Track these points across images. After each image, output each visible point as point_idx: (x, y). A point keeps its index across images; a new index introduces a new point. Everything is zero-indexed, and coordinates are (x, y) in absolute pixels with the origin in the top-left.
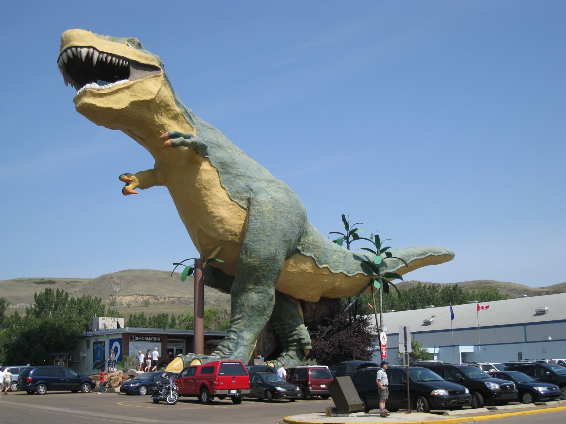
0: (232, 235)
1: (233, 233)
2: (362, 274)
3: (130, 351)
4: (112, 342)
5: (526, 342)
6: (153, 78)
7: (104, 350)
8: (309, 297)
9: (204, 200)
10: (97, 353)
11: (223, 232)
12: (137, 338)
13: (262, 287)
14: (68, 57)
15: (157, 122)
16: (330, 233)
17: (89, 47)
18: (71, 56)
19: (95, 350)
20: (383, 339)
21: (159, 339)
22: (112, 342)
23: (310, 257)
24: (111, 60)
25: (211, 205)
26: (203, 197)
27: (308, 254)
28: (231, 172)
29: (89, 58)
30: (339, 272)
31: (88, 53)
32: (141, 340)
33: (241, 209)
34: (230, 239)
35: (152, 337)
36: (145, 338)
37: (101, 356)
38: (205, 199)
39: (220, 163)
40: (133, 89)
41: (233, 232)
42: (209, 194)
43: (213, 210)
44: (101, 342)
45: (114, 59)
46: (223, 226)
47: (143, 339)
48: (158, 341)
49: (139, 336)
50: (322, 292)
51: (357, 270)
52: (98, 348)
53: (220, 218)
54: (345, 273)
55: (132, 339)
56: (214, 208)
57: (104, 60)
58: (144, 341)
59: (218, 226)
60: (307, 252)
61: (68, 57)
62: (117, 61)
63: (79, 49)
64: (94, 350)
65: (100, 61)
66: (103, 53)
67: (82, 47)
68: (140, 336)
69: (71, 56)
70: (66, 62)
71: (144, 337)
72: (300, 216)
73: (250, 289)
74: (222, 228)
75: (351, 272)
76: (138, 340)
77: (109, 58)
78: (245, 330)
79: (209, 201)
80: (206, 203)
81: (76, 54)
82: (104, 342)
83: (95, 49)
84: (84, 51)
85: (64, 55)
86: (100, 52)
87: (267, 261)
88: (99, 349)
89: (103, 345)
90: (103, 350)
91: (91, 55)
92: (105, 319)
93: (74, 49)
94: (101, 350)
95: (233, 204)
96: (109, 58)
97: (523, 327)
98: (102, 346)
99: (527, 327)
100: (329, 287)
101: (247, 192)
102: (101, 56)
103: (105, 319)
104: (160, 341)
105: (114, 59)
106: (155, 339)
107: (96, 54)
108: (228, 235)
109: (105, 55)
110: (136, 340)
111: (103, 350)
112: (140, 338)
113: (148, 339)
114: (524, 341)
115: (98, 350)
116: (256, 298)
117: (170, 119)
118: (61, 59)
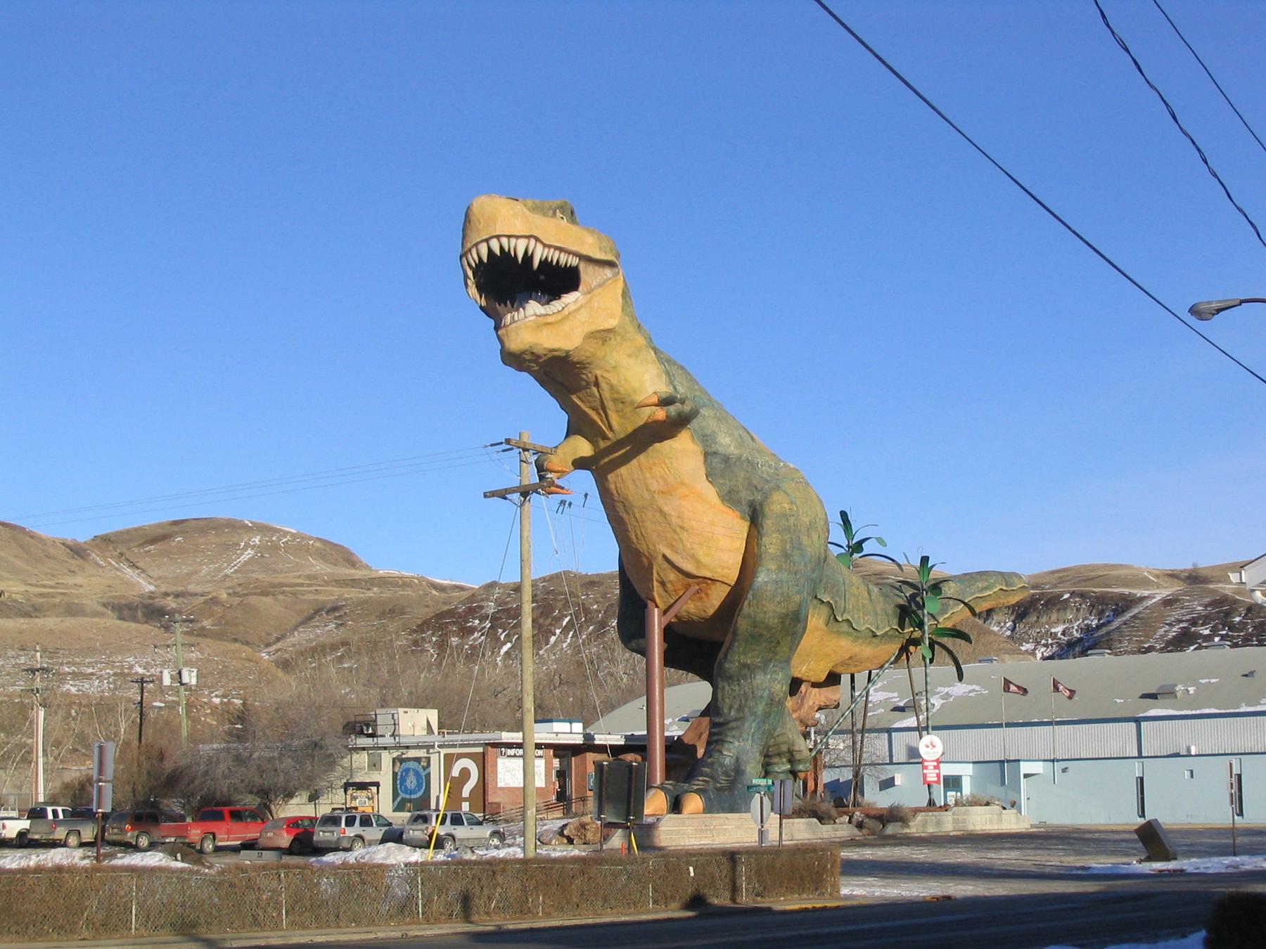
3: (499, 776)
10: (403, 780)
14: (490, 251)
18: (498, 252)
19: (399, 774)
22: (450, 760)
23: (829, 602)
29: (528, 258)
37: (419, 786)
44: (418, 760)
52: (407, 770)
62: (566, 257)
63: (513, 241)
64: (395, 774)
65: (545, 263)
69: (498, 252)
76: (510, 756)
81: (507, 250)
83: (537, 239)
86: (545, 246)
88: (411, 773)
90: (423, 774)
91: (530, 253)
93: (504, 241)
94: (417, 774)
98: (420, 767)
102: (546, 250)
110: (508, 756)
111: (423, 774)
115: (407, 774)
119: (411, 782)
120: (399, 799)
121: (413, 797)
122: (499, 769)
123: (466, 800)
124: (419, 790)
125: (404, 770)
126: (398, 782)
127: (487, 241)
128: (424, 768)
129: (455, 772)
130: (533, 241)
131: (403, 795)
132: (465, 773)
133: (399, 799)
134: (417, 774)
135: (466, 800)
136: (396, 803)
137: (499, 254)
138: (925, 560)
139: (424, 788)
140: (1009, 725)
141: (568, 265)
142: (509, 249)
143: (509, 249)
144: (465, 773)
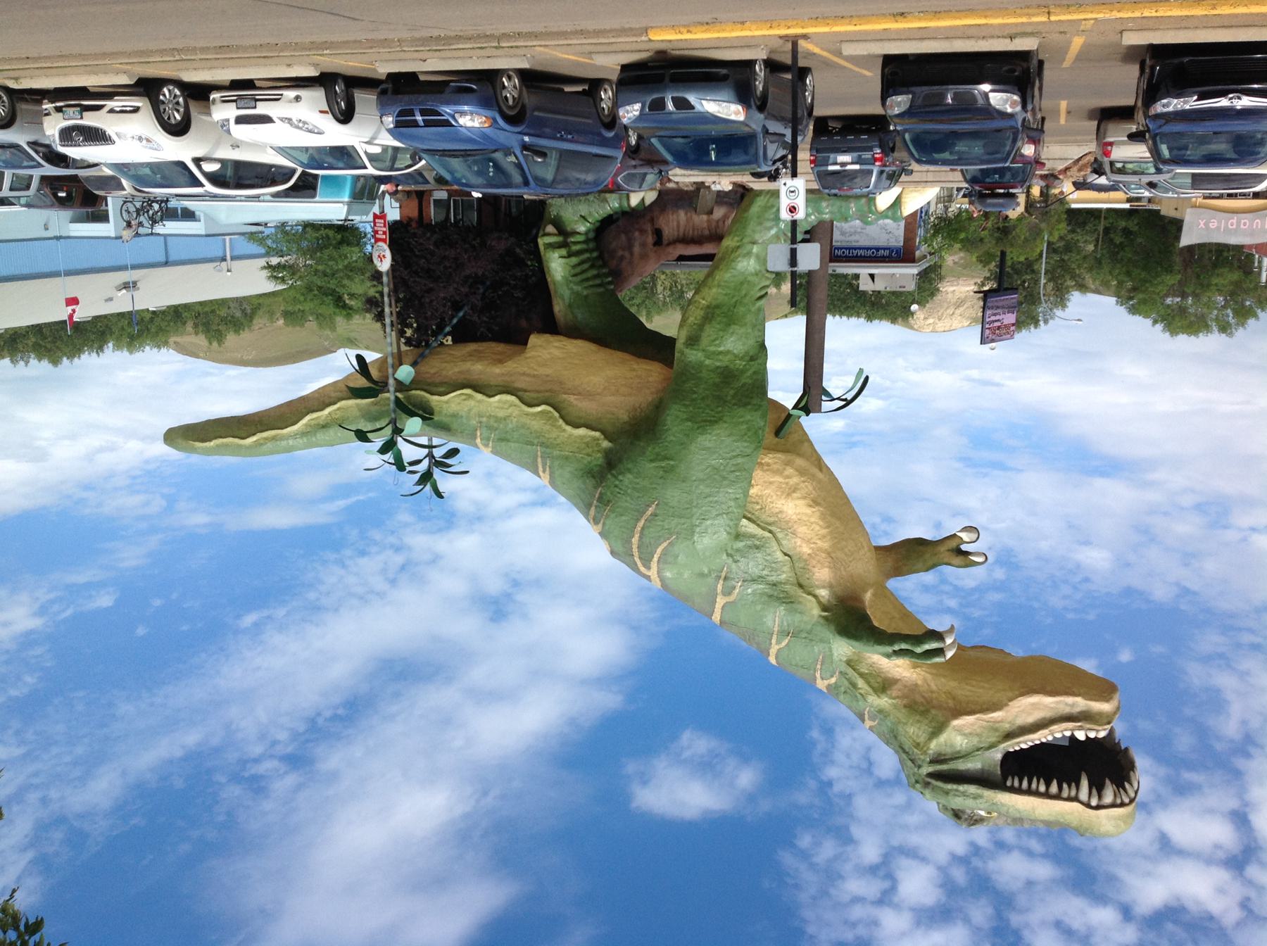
0: (768, 465)
1: (766, 468)
2: (432, 394)
6: (947, 757)
8: (556, 344)
9: (825, 528)
11: (785, 469)
12: (887, 253)
13: (718, 364)
15: (929, 673)
16: (467, 472)
17: (1098, 807)
20: (384, 256)
23: (576, 426)
24: (1048, 785)
25: (813, 520)
26: (831, 533)
27: (582, 431)
28: (767, 587)
30: (497, 398)
31: (1100, 797)
32: (878, 249)
33: (753, 517)
34: (771, 455)
36: (870, 253)
38: (824, 531)
39: (791, 602)
40: (997, 734)
41: (767, 470)
42: (818, 542)
43: (809, 511)
46: (787, 480)
47: (844, 252)
50: (528, 355)
51: (447, 402)
53: (795, 495)
54: (479, 396)
56: (806, 514)
57: (1065, 786)
58: (871, 249)
59: (795, 480)
60: (582, 437)
62: (1034, 786)
66: (1069, 799)
67: (1113, 805)
68: (881, 257)
71: (870, 257)
72: (618, 510)
73: (742, 359)
74: (788, 477)
75: (464, 397)
76: (884, 249)
77: (1025, 784)
78: (752, 275)
79: (818, 528)
80: (821, 523)
81: (1121, 789)
83: (1088, 806)
84: (1108, 797)
86: (1076, 799)
87: (714, 417)
91: (1094, 791)
92: (900, 287)
95: (770, 524)
96: (1054, 788)
100: (515, 365)
101: (738, 550)
102: (1073, 793)
103: (900, 287)
104: (835, 248)
105: (1042, 788)
107: (1084, 795)
108: (775, 463)
109: (1065, 794)
112: (881, 252)
113: (861, 252)
116: (729, 341)
117: (900, 680)
140: (69, 273)
141: (1026, 779)
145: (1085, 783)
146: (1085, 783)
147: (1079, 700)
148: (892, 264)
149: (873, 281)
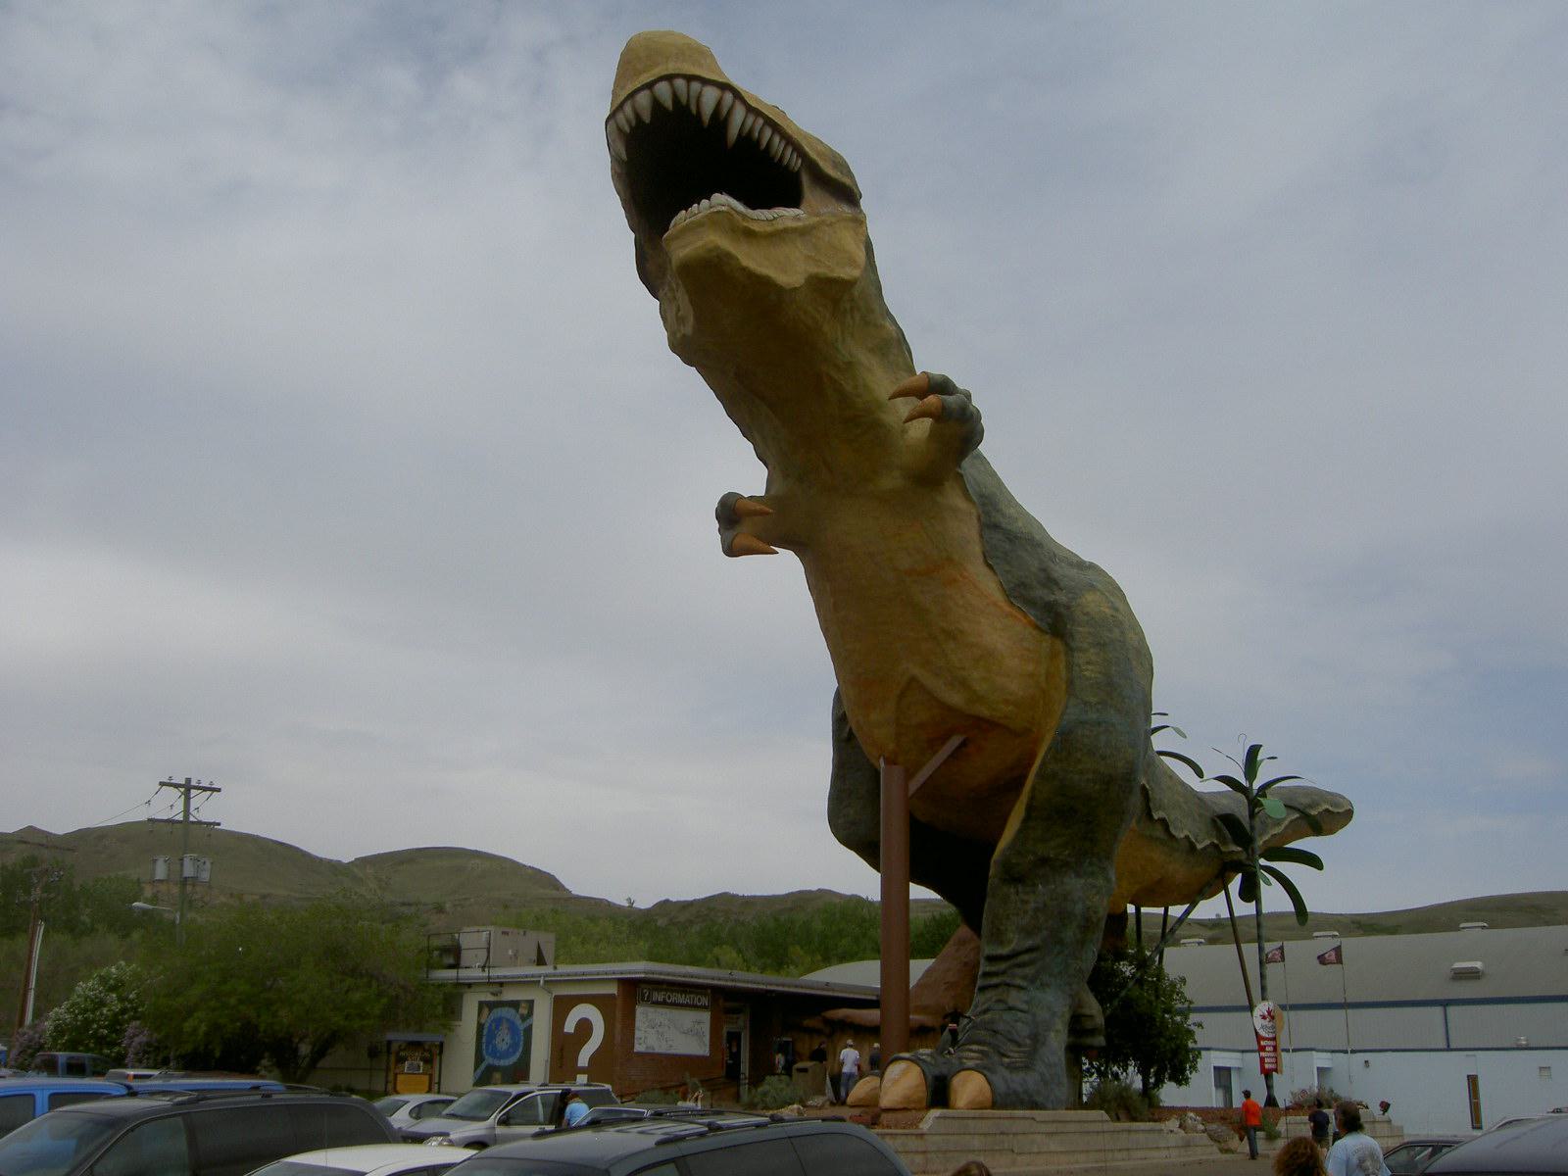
3: (638, 1034)
4: (562, 1006)
5: (1449, 1049)
7: (529, 1030)
10: (492, 1036)
14: (656, 104)
17: (725, 87)
18: (668, 103)
19: (487, 1025)
21: (705, 1001)
22: (562, 1006)
29: (720, 121)
31: (719, 104)
32: (664, 1004)
35: (690, 993)
37: (514, 1046)
44: (515, 1005)
45: (777, 139)
48: (704, 1008)
49: (659, 990)
52: (498, 1022)
55: (643, 1000)
61: (656, 104)
63: (696, 86)
64: (480, 1027)
65: (747, 140)
69: (668, 103)
70: (647, 118)
71: (672, 991)
76: (657, 1003)
81: (684, 100)
82: (531, 1003)
83: (737, 95)
84: (710, 96)
85: (643, 100)
86: (750, 109)
88: (505, 1026)
89: (523, 1011)
90: (522, 1026)
91: (724, 111)
93: (680, 83)
94: (513, 1029)
97: (1438, 1010)
98: (518, 1016)
99: (1452, 1010)
105: (777, 139)
106: (696, 1001)
107: (739, 114)
110: (653, 1003)
111: (522, 1026)
112: (659, 996)
113: (681, 999)
114: (1443, 1045)
115: (497, 1027)
118: (628, 108)
119: (503, 1040)
120: (483, 1066)
121: (504, 1063)
122: (638, 1024)
123: (583, 1071)
124: (514, 1053)
125: (494, 1020)
126: (484, 1040)
127: (650, 86)
128: (524, 1018)
129: (570, 1027)
130: (729, 97)
131: (489, 1060)
132: (585, 1026)
133: (483, 1066)
134: (513, 1029)
135: (583, 1071)
136: (479, 1071)
137: (671, 108)
138: (1253, 752)
139: (521, 1050)
142: (688, 101)
143: (688, 101)
144: (585, 1026)
145: (733, 132)
146: (733, 132)
147: (746, 262)
148: (701, 981)
149: (539, 947)
